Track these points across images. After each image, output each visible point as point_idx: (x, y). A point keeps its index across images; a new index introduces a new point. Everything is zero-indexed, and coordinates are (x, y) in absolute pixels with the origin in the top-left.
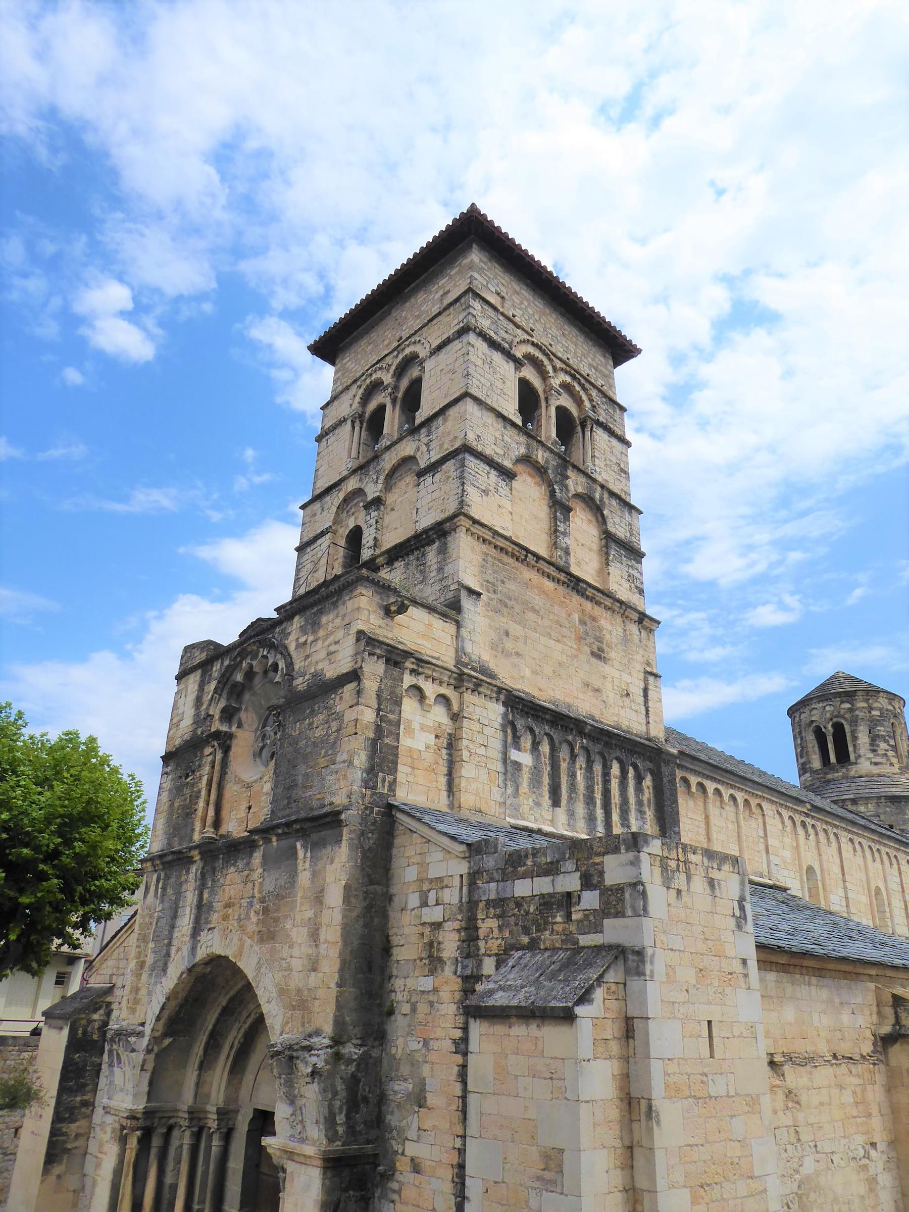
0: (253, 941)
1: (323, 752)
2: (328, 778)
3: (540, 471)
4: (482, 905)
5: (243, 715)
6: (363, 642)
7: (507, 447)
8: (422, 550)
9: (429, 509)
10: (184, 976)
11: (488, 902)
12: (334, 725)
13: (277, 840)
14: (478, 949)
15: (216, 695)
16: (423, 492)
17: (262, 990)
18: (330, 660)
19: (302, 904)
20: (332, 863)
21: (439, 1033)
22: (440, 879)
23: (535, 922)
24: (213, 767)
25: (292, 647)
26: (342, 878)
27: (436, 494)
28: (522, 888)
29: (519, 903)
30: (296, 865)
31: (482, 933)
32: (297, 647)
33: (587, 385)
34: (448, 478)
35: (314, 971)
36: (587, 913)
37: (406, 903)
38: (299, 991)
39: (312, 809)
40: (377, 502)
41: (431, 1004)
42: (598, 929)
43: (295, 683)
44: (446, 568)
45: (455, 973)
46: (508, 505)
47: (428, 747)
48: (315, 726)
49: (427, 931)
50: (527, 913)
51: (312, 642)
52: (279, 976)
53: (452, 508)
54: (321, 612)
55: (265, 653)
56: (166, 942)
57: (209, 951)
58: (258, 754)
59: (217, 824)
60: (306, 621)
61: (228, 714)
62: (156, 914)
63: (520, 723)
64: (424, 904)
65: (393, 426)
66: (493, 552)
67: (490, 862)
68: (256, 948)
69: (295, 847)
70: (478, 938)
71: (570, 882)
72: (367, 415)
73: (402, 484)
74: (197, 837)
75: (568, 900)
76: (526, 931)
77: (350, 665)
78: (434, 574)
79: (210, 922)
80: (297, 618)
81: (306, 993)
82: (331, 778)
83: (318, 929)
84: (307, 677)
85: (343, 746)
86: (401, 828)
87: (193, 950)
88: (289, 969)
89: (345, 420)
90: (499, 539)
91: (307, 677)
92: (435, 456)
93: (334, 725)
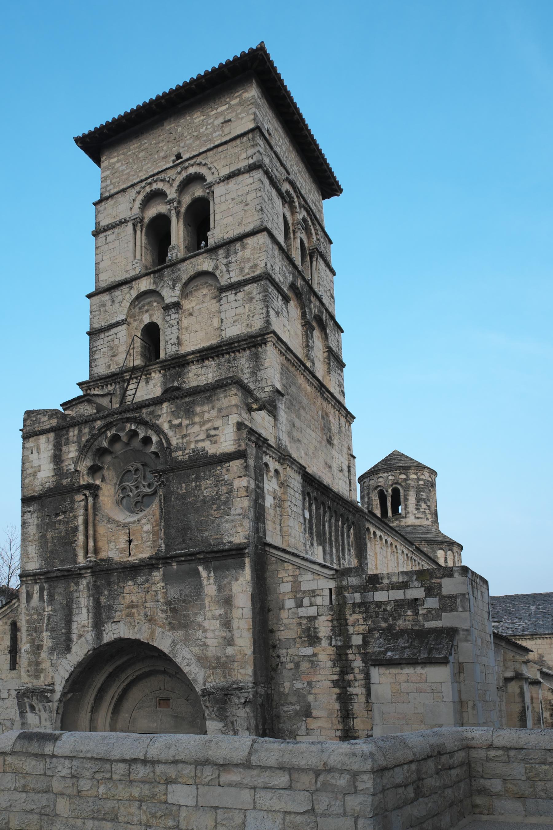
1: (215, 507)
2: (224, 525)
3: (298, 295)
5: (106, 473)
6: (245, 433)
7: (284, 276)
8: (233, 355)
9: (234, 322)
10: (90, 653)
12: (224, 489)
13: (177, 565)
15: (82, 456)
16: (225, 307)
18: (211, 441)
20: (237, 580)
24: (86, 510)
25: (165, 427)
26: (248, 589)
27: (240, 310)
32: (170, 427)
33: (316, 222)
34: (252, 299)
35: (230, 645)
37: (283, 605)
39: (210, 545)
40: (177, 306)
43: (174, 455)
44: (259, 373)
46: (286, 323)
47: (271, 506)
48: (203, 487)
51: (187, 426)
52: (195, 650)
53: (258, 324)
54: (194, 403)
55: (133, 427)
57: (116, 636)
58: (119, 502)
59: (96, 551)
60: (177, 407)
61: (94, 470)
62: (46, 613)
63: (308, 489)
64: (300, 605)
65: (178, 238)
66: (285, 362)
72: (146, 221)
73: (199, 294)
74: (81, 560)
77: (233, 447)
78: (247, 375)
79: (113, 618)
80: (165, 405)
82: (227, 525)
83: (230, 621)
84: (187, 451)
85: (236, 504)
86: (273, 559)
87: (99, 635)
89: (125, 221)
90: (289, 352)
91: (187, 451)
92: (235, 278)
93: (224, 489)
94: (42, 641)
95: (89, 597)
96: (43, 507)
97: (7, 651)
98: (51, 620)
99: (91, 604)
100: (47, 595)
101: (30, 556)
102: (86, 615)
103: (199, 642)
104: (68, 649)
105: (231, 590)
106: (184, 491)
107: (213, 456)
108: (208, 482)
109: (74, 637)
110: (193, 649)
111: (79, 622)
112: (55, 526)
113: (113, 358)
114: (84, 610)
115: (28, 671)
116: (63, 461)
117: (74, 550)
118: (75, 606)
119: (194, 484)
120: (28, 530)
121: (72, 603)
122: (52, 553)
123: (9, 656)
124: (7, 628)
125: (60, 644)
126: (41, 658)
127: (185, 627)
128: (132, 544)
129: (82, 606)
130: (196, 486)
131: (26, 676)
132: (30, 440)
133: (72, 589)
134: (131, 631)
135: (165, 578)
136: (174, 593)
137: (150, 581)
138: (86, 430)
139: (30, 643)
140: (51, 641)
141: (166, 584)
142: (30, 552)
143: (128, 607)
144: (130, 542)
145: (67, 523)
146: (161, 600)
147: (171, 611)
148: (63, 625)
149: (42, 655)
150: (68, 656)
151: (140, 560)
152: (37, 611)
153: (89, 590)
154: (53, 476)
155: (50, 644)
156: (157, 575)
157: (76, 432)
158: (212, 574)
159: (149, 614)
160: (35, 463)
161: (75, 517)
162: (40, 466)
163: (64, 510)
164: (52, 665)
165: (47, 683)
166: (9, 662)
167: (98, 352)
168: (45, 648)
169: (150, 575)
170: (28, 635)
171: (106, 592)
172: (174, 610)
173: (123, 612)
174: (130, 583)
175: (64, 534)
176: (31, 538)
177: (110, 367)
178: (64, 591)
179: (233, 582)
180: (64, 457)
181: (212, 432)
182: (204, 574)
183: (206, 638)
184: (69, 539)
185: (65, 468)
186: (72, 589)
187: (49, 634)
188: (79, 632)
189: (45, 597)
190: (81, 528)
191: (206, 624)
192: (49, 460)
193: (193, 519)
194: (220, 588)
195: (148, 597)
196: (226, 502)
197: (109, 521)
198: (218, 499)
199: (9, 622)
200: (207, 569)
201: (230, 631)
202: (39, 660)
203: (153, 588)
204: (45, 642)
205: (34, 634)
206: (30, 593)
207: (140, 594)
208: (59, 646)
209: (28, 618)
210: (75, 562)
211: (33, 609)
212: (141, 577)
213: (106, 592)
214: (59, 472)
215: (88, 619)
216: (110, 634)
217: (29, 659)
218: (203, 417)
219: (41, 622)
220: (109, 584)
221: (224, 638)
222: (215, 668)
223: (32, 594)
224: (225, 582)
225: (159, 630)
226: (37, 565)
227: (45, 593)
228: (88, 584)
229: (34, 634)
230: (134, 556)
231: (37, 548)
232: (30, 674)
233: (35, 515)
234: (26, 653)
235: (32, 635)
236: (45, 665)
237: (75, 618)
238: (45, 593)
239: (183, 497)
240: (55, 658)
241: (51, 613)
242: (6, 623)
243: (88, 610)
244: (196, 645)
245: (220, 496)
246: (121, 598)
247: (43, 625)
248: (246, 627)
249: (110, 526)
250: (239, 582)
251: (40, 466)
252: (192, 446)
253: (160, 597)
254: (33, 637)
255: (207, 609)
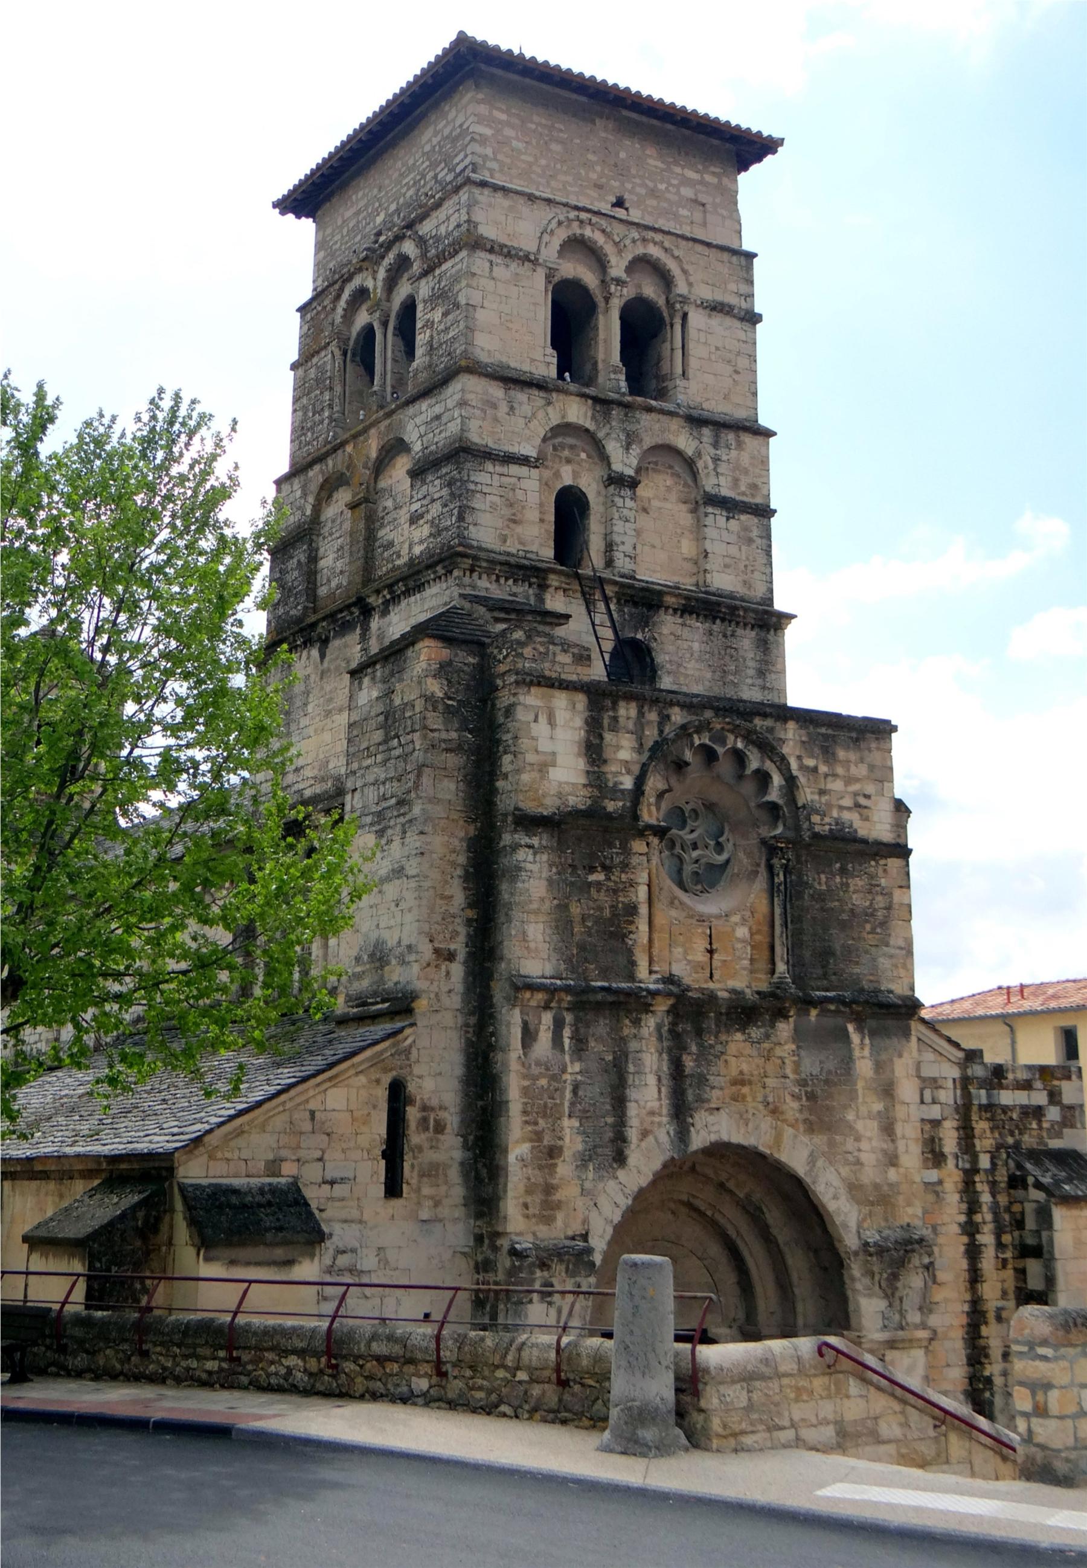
0: (797, 1130)
1: (868, 927)
4: (975, 1108)
11: (980, 1106)
14: (974, 1145)
17: (823, 1186)
18: (861, 815)
19: (864, 1096)
21: (946, 1218)
22: (935, 1080)
23: (1017, 1127)
28: (1006, 1097)
29: (1005, 1109)
30: (850, 1051)
31: (977, 1132)
36: (1053, 1123)
38: (877, 1186)
41: (937, 1193)
42: (1059, 1135)
45: (957, 1166)
49: (927, 1127)
50: (1011, 1119)
51: (826, 776)
56: (610, 1120)
67: (977, 1071)
68: (805, 1139)
69: (846, 1030)
70: (974, 1137)
71: (1039, 1098)
75: (1038, 1112)
76: (1012, 1134)
80: (791, 725)
81: (886, 1188)
88: (858, 1162)
94: (560, 1138)
95: (660, 1054)
96: (561, 846)
97: (378, 1152)
98: (581, 1093)
99: (665, 1069)
100: (571, 1038)
101: (532, 945)
102: (655, 1090)
103: (851, 1158)
104: (620, 1159)
105: (893, 1071)
106: (824, 887)
107: (864, 841)
108: (860, 883)
109: (632, 1134)
110: (842, 1170)
111: (642, 1103)
112: (589, 892)
113: (512, 525)
114: (652, 1080)
115: (526, 1206)
116: (605, 761)
117: (630, 952)
118: (631, 1068)
119: (838, 879)
120: (526, 885)
121: (627, 1061)
122: (582, 947)
123: (383, 1163)
124: (382, 1094)
125: (601, 1146)
126: (558, 1176)
127: (829, 1129)
128: (716, 956)
129: (647, 1070)
130: (842, 884)
131: (521, 1218)
132: (533, 690)
133: (626, 1032)
134: (742, 1131)
135: (798, 1036)
136: (812, 1064)
137: (773, 1039)
138: (653, 716)
139: (531, 1140)
140: (579, 1139)
141: (798, 1047)
142: (531, 937)
143: (735, 1082)
144: (711, 952)
145: (615, 891)
146: (791, 1076)
147: (808, 1099)
148: (608, 1107)
149: (558, 1170)
150: (621, 1173)
151: (733, 991)
152: (547, 1069)
153: (660, 1038)
154: (585, 786)
155: (580, 1147)
156: (784, 1029)
157: (633, 712)
158: (867, 1041)
159: (770, 1099)
160: (544, 746)
161: (632, 884)
162: (554, 754)
163: (608, 862)
164: (583, 1192)
165: (570, 1233)
166: (382, 1179)
167: (478, 495)
168: (567, 1154)
169: (773, 1026)
170: (526, 1122)
171: (694, 1048)
172: (812, 1097)
173: (727, 1091)
174: (739, 1036)
175: (607, 913)
176: (534, 906)
177: (505, 541)
178: (608, 1034)
179: (895, 1059)
180: (608, 754)
181: (863, 801)
182: (855, 1038)
183: (859, 1150)
184: (619, 926)
185: (609, 776)
186: (626, 1032)
187: (577, 1124)
188: (642, 1123)
189: (567, 1042)
190: (643, 910)
191: (859, 1126)
192: (576, 750)
193: (839, 940)
194: (879, 1066)
195: (770, 1067)
196: (883, 924)
197: (672, 903)
198: (872, 915)
199: (387, 1079)
200: (860, 1029)
201: (893, 1141)
202: (554, 1182)
203: (778, 1052)
204: (567, 1139)
205: (541, 1121)
206: (532, 1027)
207: (757, 1060)
208: (599, 1150)
209: (526, 1083)
210: (632, 977)
211: (538, 1063)
212: (758, 1027)
213: (694, 1048)
214: (597, 780)
215: (660, 1099)
216: (703, 1133)
217: (529, 1179)
218: (848, 770)
219: (557, 1095)
220: (699, 1032)
221: (885, 1152)
222: (872, 1204)
223: (537, 1031)
224: (884, 1057)
225: (789, 1131)
226: (549, 970)
227: (567, 1032)
228: (659, 1027)
229: (541, 1121)
230: (719, 981)
231: (548, 931)
232: (531, 1211)
233: (545, 857)
234: (521, 1164)
235: (536, 1123)
236: (568, 1192)
237: (632, 1094)
238: (567, 1032)
239: (820, 897)
240: (591, 1175)
241: (579, 1077)
242: (378, 1081)
243: (659, 1080)
244: (847, 1163)
245: (875, 910)
246: (721, 1063)
247: (562, 1104)
248: (913, 1136)
249: (673, 913)
250: (903, 1060)
251: (554, 754)
252: (835, 814)
253: (788, 1071)
254: (539, 1128)
255: (860, 1100)
